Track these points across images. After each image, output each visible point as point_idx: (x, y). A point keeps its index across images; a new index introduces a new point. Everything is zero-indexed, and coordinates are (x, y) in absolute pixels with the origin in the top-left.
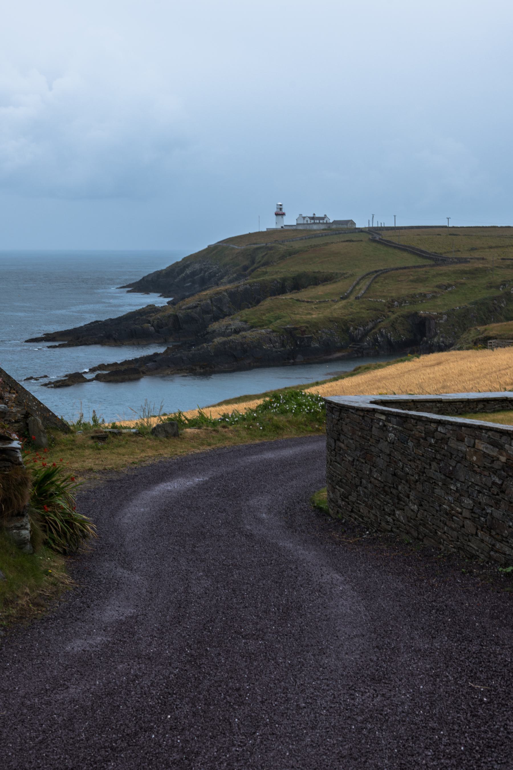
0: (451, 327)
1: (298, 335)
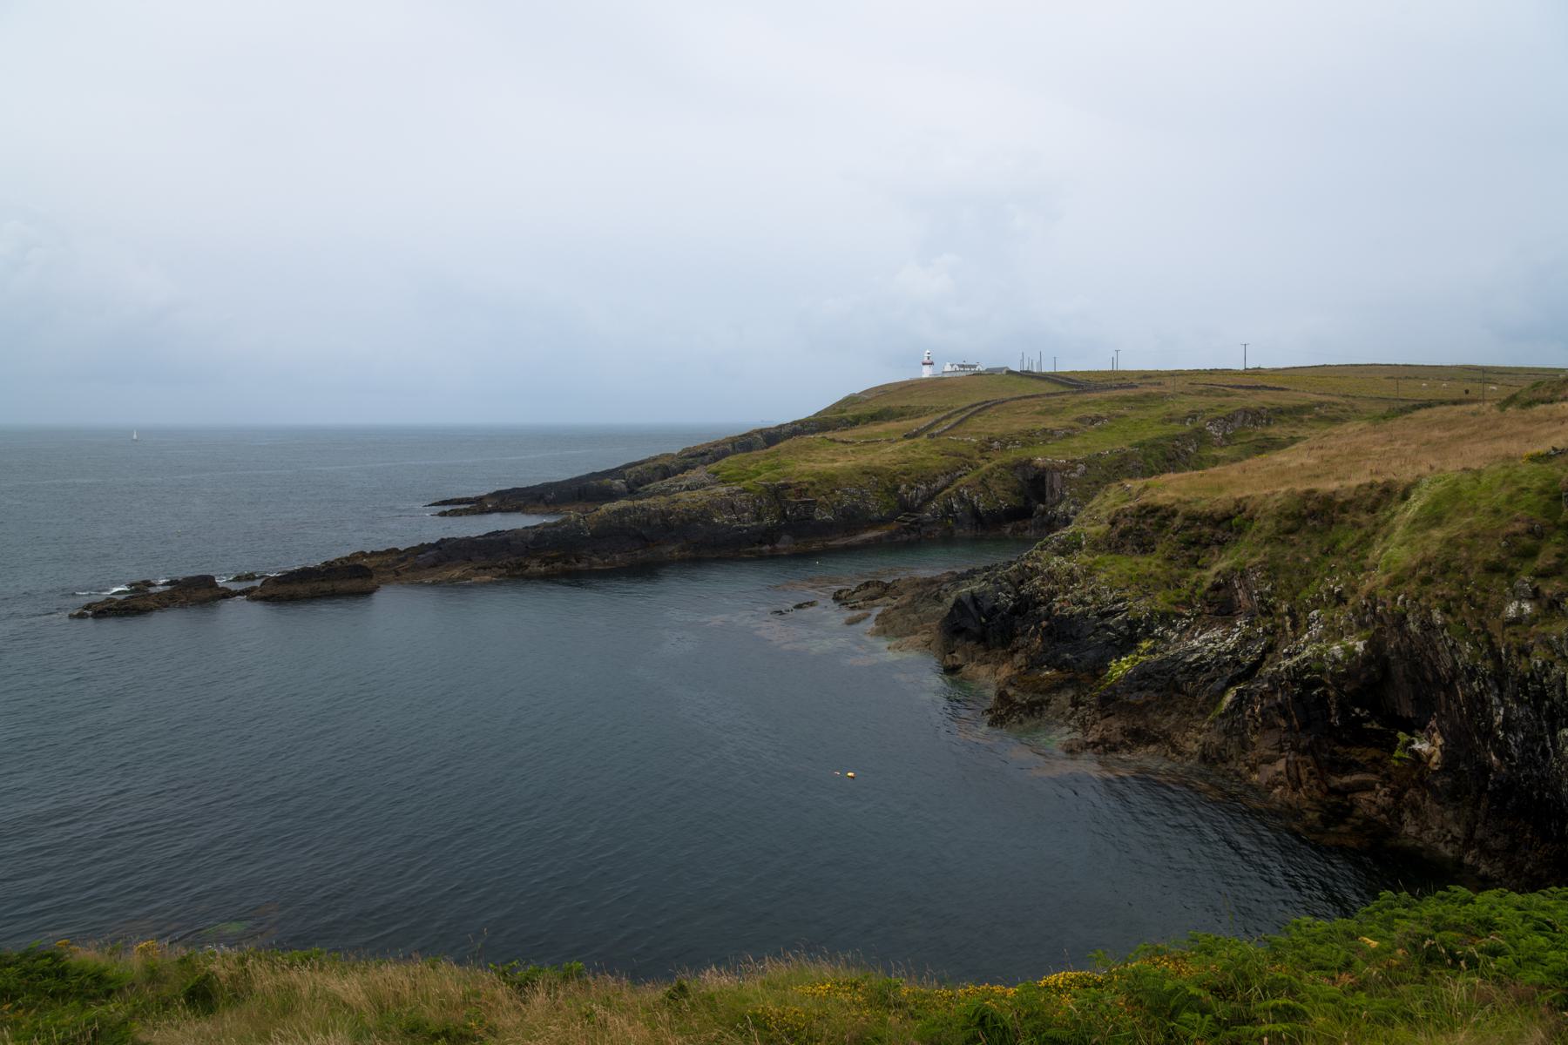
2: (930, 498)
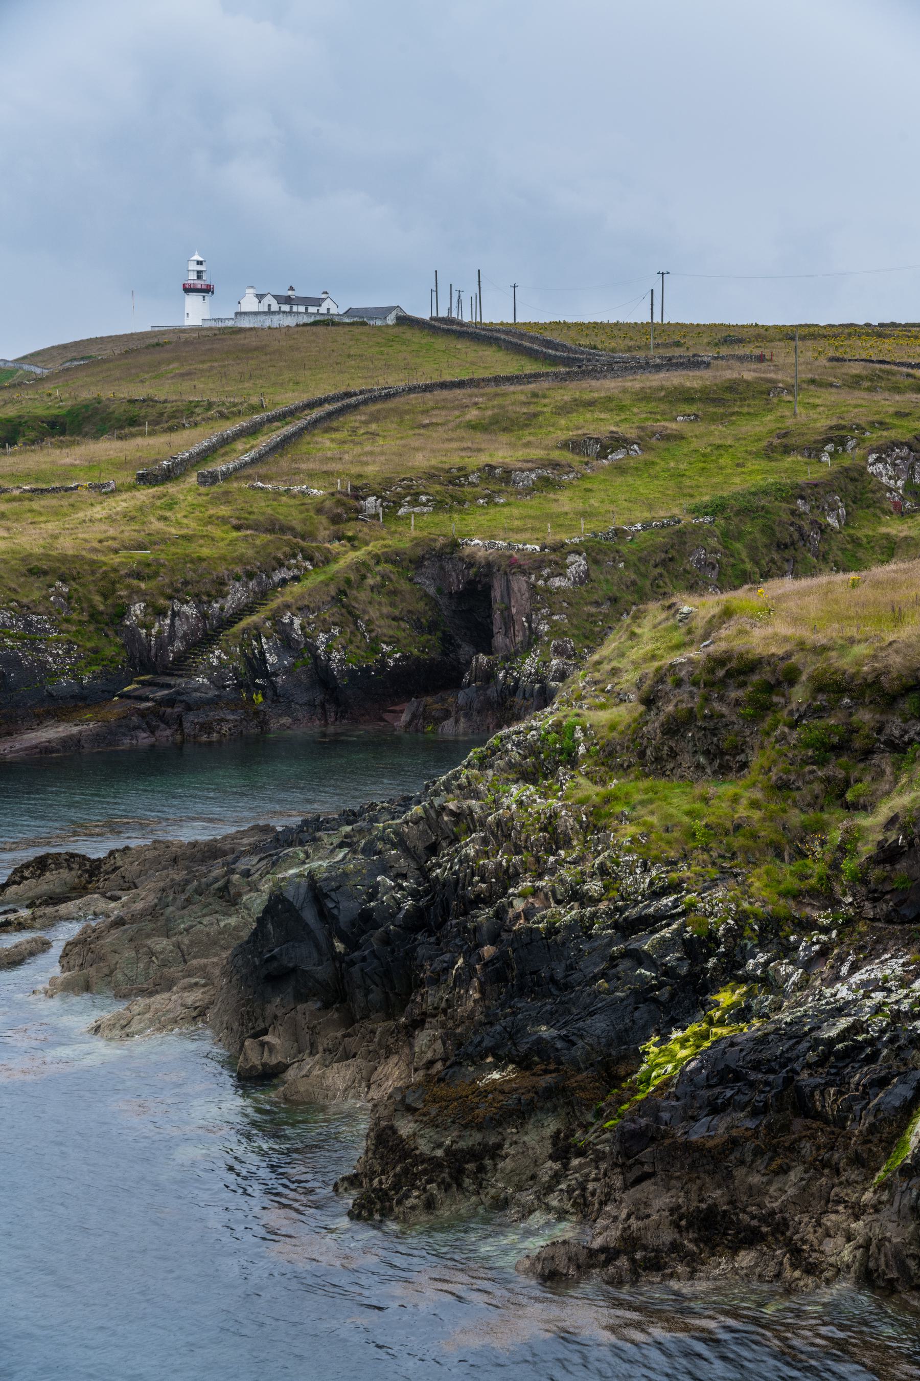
0: (605, 608)
2: (205, 638)
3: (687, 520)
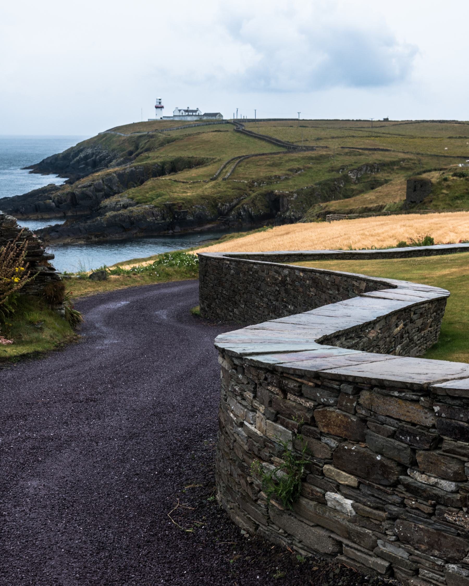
0: (300, 203)
1: (175, 210)
3: (315, 186)
